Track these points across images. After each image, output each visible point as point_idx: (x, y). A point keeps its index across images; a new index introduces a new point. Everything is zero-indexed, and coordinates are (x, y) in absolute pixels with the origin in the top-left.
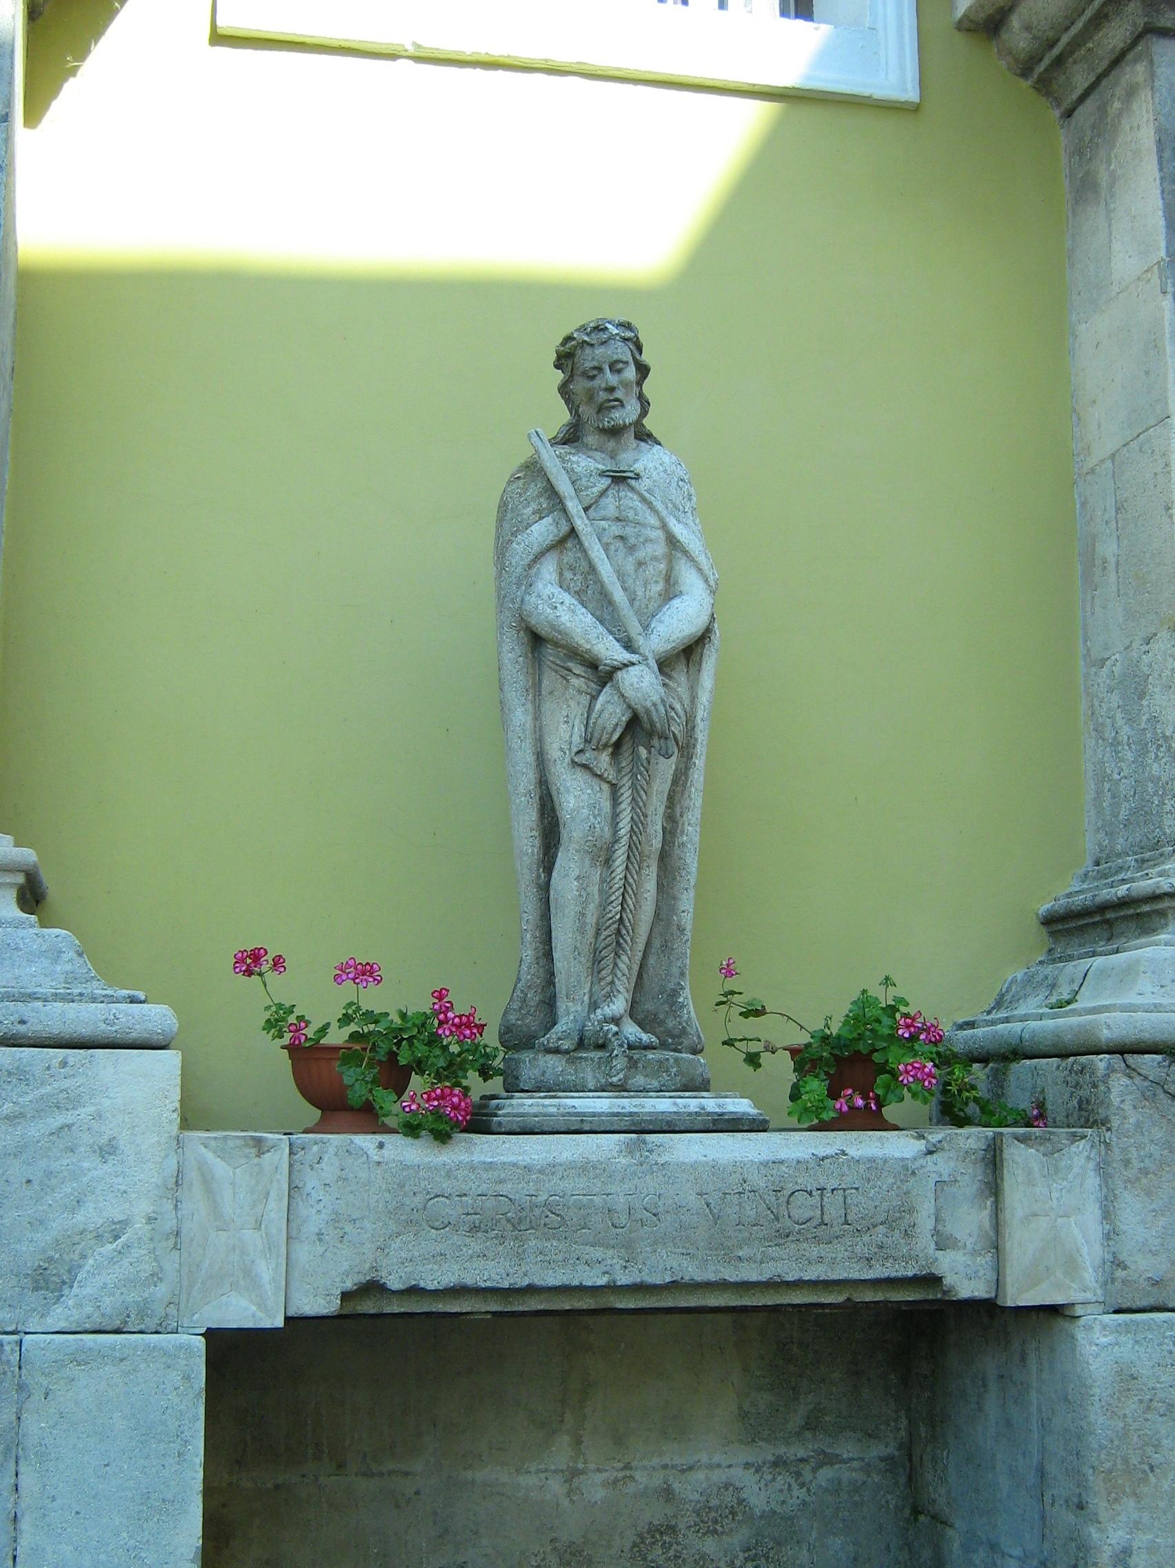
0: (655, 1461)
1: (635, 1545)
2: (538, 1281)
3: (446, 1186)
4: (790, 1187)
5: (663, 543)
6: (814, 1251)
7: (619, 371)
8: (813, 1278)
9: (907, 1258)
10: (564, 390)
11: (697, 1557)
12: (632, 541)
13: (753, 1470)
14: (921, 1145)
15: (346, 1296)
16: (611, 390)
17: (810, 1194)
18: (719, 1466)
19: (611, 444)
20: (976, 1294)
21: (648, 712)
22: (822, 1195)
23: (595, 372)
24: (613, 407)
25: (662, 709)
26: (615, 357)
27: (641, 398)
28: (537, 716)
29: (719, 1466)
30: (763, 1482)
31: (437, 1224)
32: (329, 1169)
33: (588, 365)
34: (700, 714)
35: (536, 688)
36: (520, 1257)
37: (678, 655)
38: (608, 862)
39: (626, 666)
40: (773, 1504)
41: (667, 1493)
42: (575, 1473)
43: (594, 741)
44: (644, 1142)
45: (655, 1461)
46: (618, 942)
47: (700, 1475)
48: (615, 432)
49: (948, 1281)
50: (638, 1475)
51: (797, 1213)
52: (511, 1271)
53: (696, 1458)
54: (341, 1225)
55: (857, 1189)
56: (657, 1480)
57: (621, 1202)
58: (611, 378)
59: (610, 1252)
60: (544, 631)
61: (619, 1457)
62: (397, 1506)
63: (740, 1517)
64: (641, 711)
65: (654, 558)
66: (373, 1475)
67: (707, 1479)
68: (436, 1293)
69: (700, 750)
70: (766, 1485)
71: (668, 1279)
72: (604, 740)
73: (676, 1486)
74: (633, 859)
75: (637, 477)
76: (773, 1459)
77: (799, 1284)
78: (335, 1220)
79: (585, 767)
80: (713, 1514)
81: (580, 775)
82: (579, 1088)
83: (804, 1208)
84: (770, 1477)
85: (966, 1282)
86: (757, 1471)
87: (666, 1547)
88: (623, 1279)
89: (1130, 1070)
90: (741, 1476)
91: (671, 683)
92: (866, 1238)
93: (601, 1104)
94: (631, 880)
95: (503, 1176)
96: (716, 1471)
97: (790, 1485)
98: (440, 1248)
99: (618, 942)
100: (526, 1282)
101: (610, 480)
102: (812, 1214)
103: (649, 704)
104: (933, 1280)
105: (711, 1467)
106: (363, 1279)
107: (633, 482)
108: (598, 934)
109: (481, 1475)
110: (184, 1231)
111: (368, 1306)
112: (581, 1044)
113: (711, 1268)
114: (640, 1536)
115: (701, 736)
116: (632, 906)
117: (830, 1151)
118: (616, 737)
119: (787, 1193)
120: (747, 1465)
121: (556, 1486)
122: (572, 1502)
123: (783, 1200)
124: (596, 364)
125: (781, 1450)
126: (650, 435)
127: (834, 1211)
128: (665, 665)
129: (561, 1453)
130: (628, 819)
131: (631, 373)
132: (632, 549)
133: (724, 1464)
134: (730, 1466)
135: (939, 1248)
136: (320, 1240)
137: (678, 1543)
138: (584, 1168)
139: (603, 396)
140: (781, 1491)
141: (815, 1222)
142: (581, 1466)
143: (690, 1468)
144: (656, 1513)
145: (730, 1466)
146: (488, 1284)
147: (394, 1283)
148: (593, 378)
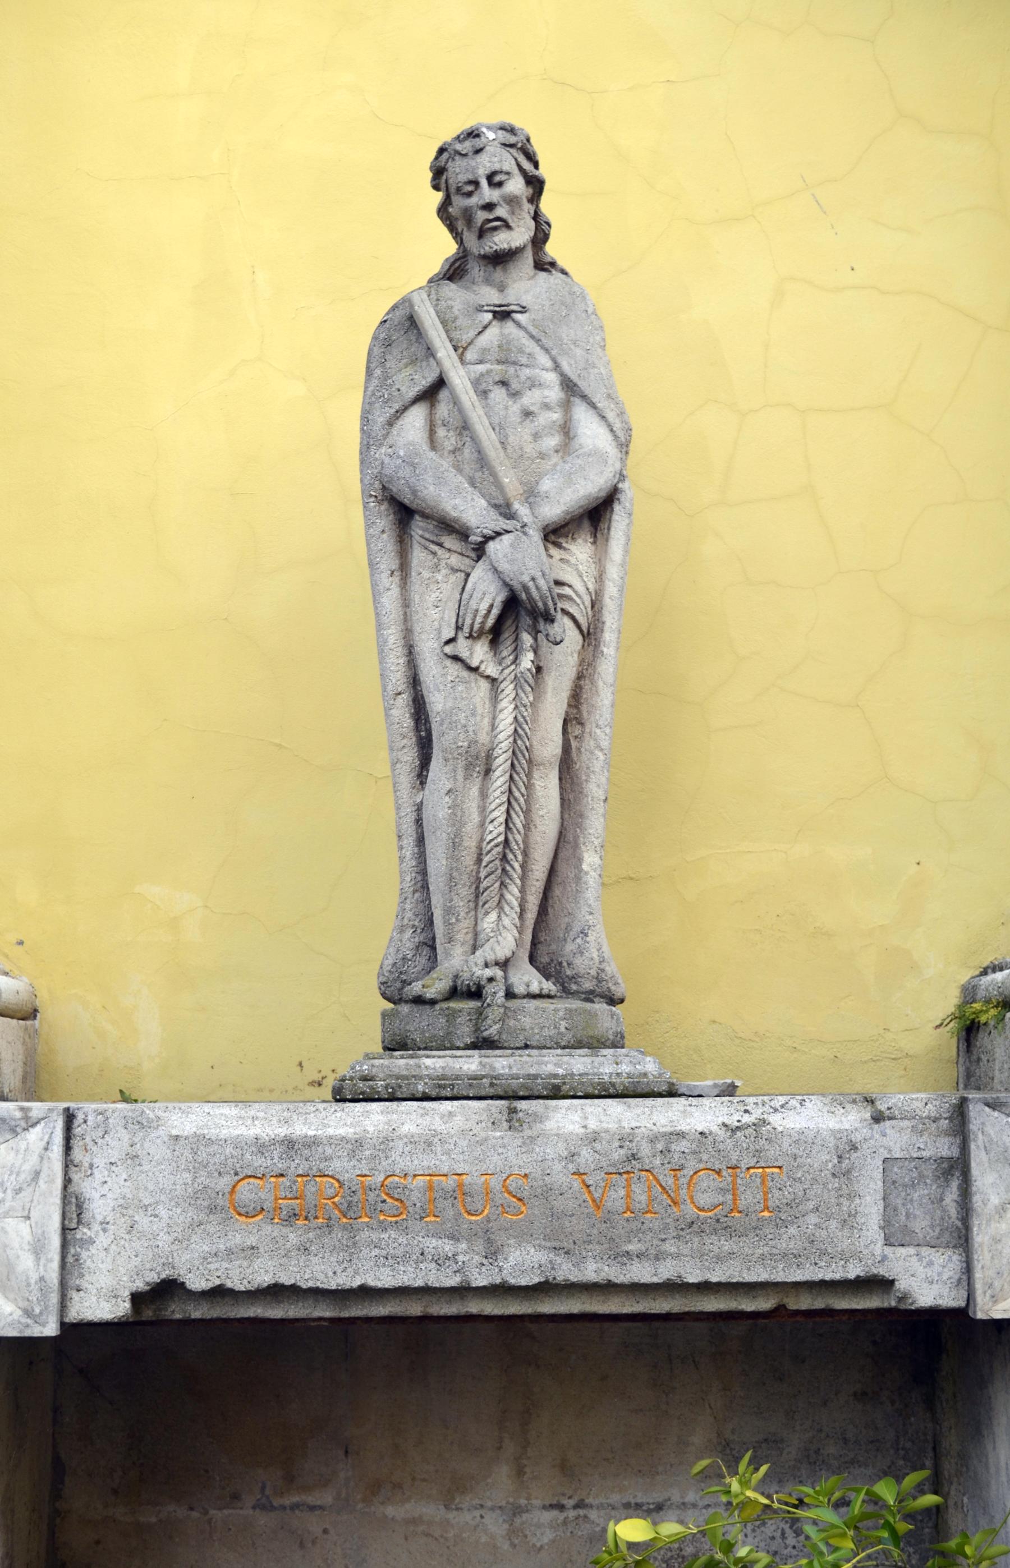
2: (372, 1282)
4: (691, 1165)
5: (557, 388)
7: (500, 184)
8: (723, 1279)
10: (443, 211)
12: (515, 385)
16: (489, 207)
17: (719, 1172)
18: (694, 1506)
19: (498, 274)
21: (526, 588)
22: (735, 1176)
23: (470, 188)
24: (495, 229)
25: (542, 582)
26: (497, 167)
27: (536, 216)
28: (406, 604)
29: (694, 1506)
31: (243, 1211)
33: (463, 178)
34: (611, 590)
35: (404, 567)
38: (488, 771)
39: (498, 534)
42: (517, 1511)
43: (467, 629)
44: (513, 1111)
45: (615, 1498)
46: (504, 870)
48: (501, 259)
49: (901, 1285)
51: (705, 1199)
54: (130, 1212)
55: (780, 1167)
58: (488, 194)
59: (463, 1246)
60: (407, 499)
61: (570, 1493)
62: (302, 1545)
64: (517, 587)
65: (547, 406)
66: (273, 1508)
69: (609, 636)
70: (754, 1531)
71: (536, 1280)
72: (477, 626)
74: (518, 768)
75: (524, 310)
77: (705, 1287)
78: (123, 1207)
79: (456, 658)
81: (454, 669)
82: (444, 1044)
83: (708, 1193)
88: (480, 1280)
91: (567, 557)
92: (792, 1230)
94: (517, 794)
97: (783, 1533)
98: (252, 1241)
99: (504, 870)
100: (356, 1283)
101: (490, 316)
102: (721, 1199)
103: (526, 578)
104: (883, 1284)
106: (154, 1278)
107: (518, 317)
108: (479, 861)
111: (176, 1311)
112: (454, 993)
115: (610, 619)
116: (519, 826)
118: (490, 622)
119: (688, 1172)
121: (495, 1525)
122: (513, 1546)
123: (683, 1181)
124: (471, 177)
126: (553, 264)
127: (748, 1198)
128: (555, 534)
130: (510, 719)
131: (516, 185)
132: (515, 395)
133: (701, 1504)
135: (888, 1243)
136: (105, 1230)
139: (481, 216)
140: (773, 1538)
141: (727, 1209)
142: (523, 1502)
146: (311, 1284)
147: (197, 1283)
148: (469, 194)
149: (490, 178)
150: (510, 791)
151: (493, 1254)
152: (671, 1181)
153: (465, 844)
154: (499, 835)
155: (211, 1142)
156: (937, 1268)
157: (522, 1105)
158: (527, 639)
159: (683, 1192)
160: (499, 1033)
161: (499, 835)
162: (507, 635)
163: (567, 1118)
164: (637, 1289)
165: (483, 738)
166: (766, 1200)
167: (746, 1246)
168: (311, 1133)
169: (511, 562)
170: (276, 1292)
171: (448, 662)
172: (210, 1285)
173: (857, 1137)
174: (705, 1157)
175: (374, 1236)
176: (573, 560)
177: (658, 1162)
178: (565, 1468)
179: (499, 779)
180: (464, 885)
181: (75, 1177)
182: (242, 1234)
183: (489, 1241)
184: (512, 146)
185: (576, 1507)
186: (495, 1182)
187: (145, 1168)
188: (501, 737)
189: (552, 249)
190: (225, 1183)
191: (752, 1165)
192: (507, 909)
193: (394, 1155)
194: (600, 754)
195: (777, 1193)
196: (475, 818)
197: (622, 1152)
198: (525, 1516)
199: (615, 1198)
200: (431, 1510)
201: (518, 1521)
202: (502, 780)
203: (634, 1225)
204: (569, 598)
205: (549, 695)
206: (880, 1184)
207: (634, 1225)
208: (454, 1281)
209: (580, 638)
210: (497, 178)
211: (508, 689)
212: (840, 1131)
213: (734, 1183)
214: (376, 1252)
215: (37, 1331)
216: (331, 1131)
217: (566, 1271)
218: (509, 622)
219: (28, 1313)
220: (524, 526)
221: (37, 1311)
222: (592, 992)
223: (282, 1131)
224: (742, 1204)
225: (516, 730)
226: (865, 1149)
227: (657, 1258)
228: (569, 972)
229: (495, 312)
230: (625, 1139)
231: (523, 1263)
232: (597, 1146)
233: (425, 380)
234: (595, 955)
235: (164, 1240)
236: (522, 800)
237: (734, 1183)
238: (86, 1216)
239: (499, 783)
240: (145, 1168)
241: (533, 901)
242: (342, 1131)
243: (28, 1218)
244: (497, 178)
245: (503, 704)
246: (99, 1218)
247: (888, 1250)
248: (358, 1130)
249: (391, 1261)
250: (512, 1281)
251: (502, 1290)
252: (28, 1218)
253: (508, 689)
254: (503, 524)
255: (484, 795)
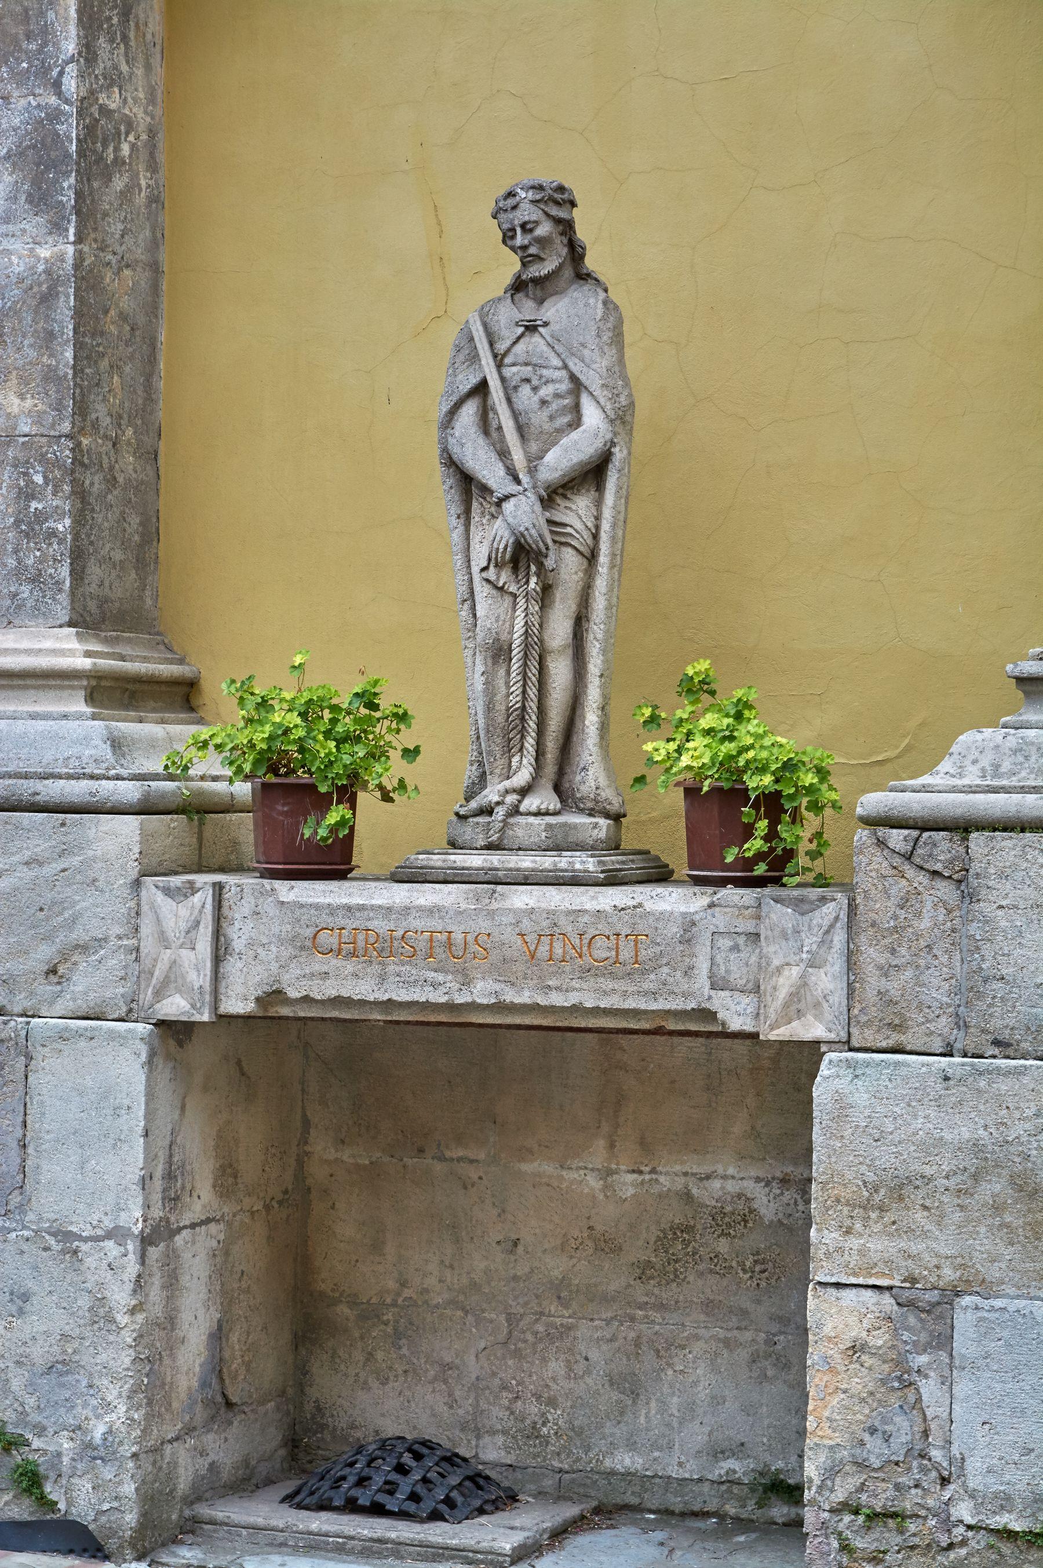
0: (678, 1168)
1: (659, 1239)
3: (330, 921)
4: (592, 932)
6: (609, 984)
7: (531, 230)
9: (685, 995)
11: (712, 1255)
13: (763, 1184)
14: (705, 901)
15: (258, 999)
17: (608, 938)
18: (733, 1177)
20: (745, 1028)
22: (617, 939)
24: (530, 262)
26: (527, 218)
29: (733, 1177)
30: (772, 1196)
31: (320, 950)
32: (245, 907)
34: (606, 526)
36: (382, 978)
37: (587, 473)
40: (781, 1216)
41: (687, 1197)
42: (610, 1172)
45: (678, 1168)
46: (523, 726)
47: (717, 1184)
50: (662, 1179)
52: (376, 989)
53: (712, 1169)
56: (680, 1183)
57: (458, 937)
59: (450, 977)
61: (646, 1162)
62: (465, 1188)
63: (750, 1225)
66: (446, 1160)
67: (723, 1188)
68: (322, 1002)
69: (603, 559)
70: (775, 1198)
71: (493, 1001)
73: (695, 1191)
75: (546, 324)
76: (781, 1177)
77: (596, 1011)
78: (249, 945)
80: (727, 1219)
83: (602, 950)
84: (778, 1191)
85: (736, 1016)
86: (767, 1185)
87: (686, 1243)
88: (459, 1000)
89: (881, 843)
90: (750, 1187)
92: (652, 976)
93: (475, 860)
94: (530, 675)
95: (371, 915)
96: (730, 1181)
98: (325, 968)
102: (608, 954)
103: (522, 529)
104: (709, 1015)
105: (724, 1177)
106: (267, 989)
107: (541, 329)
109: (526, 1167)
110: (142, 949)
113: (527, 993)
114: (663, 1231)
115: (604, 547)
117: (631, 903)
118: (508, 556)
119: (588, 936)
120: (758, 1180)
121: (594, 1182)
123: (586, 942)
125: (789, 1169)
126: (588, 275)
127: (626, 954)
129: (598, 1154)
130: (522, 623)
132: (535, 389)
134: (742, 1179)
137: (695, 1241)
138: (432, 911)
140: (788, 1205)
141: (611, 961)
142: (614, 1166)
143: (708, 1177)
144: (675, 1214)
145: (742, 1179)
146: (359, 997)
147: (293, 994)
149: (523, 226)
150: (525, 673)
151: (467, 982)
152: (578, 941)
153: (497, 708)
154: (517, 702)
155: (302, 906)
156: (743, 1006)
157: (499, 888)
158: (533, 568)
159: (585, 949)
160: (500, 839)
161: (517, 702)
162: (522, 564)
163: (522, 898)
164: (552, 1010)
165: (504, 637)
166: (637, 956)
167: (620, 985)
168: (361, 902)
169: (515, 517)
170: (338, 1001)
171: (484, 583)
172: (301, 995)
173: (697, 917)
174: (600, 927)
175: (397, 969)
176: (574, 507)
177: (570, 929)
178: (645, 1145)
179: (516, 665)
180: (498, 736)
181: (224, 925)
182: (319, 963)
183: (466, 976)
184: (538, 201)
185: (650, 1172)
186: (470, 938)
187: (264, 921)
188: (515, 636)
189: (591, 262)
190: (309, 932)
191: (629, 932)
192: (525, 753)
193: (411, 919)
194: (596, 643)
195: (644, 952)
196: (503, 690)
197: (548, 921)
198: (615, 1177)
199: (543, 951)
200: (548, 1168)
201: (609, 1179)
202: (517, 665)
203: (555, 969)
204: (571, 535)
205: (557, 604)
206: (709, 948)
207: (555, 969)
208: (443, 1000)
209: (585, 560)
210: (528, 227)
211: (521, 602)
212: (687, 913)
213: (617, 944)
214: (398, 979)
215: (197, 1018)
216: (374, 902)
217: (511, 996)
218: (523, 555)
219: (193, 1006)
220: (526, 490)
221: (198, 1005)
222: (592, 809)
223: (345, 901)
224: (621, 958)
225: (527, 631)
226: (701, 925)
227: (567, 991)
228: (578, 796)
229: (527, 327)
230: (550, 913)
231: (482, 991)
232: (533, 917)
233: (474, 380)
234: (593, 784)
235: (274, 967)
236: (534, 679)
237: (617, 944)
238: (230, 950)
239: (515, 667)
240: (264, 921)
241: (552, 746)
242: (379, 902)
243: (194, 949)
244: (528, 227)
245: (517, 613)
246: (237, 951)
247: (713, 993)
248: (390, 901)
249: (407, 985)
250: (479, 1001)
251: (473, 1007)
252: (194, 949)
253: (521, 602)
254: (514, 488)
255: (508, 673)
